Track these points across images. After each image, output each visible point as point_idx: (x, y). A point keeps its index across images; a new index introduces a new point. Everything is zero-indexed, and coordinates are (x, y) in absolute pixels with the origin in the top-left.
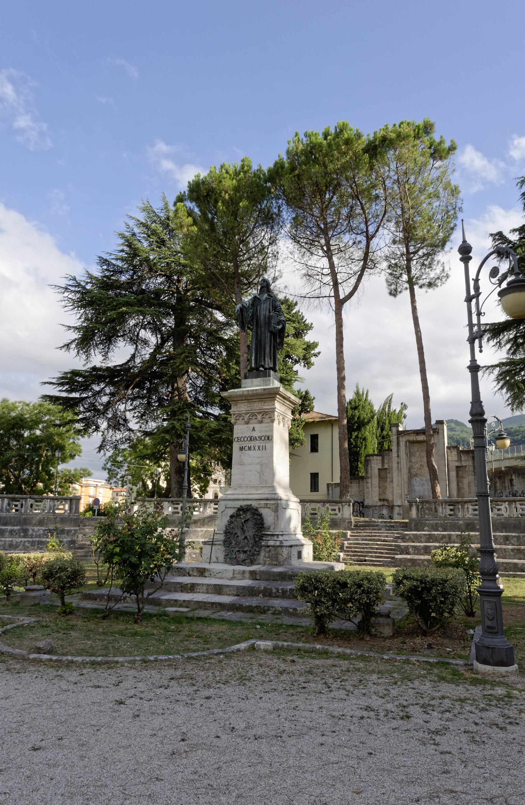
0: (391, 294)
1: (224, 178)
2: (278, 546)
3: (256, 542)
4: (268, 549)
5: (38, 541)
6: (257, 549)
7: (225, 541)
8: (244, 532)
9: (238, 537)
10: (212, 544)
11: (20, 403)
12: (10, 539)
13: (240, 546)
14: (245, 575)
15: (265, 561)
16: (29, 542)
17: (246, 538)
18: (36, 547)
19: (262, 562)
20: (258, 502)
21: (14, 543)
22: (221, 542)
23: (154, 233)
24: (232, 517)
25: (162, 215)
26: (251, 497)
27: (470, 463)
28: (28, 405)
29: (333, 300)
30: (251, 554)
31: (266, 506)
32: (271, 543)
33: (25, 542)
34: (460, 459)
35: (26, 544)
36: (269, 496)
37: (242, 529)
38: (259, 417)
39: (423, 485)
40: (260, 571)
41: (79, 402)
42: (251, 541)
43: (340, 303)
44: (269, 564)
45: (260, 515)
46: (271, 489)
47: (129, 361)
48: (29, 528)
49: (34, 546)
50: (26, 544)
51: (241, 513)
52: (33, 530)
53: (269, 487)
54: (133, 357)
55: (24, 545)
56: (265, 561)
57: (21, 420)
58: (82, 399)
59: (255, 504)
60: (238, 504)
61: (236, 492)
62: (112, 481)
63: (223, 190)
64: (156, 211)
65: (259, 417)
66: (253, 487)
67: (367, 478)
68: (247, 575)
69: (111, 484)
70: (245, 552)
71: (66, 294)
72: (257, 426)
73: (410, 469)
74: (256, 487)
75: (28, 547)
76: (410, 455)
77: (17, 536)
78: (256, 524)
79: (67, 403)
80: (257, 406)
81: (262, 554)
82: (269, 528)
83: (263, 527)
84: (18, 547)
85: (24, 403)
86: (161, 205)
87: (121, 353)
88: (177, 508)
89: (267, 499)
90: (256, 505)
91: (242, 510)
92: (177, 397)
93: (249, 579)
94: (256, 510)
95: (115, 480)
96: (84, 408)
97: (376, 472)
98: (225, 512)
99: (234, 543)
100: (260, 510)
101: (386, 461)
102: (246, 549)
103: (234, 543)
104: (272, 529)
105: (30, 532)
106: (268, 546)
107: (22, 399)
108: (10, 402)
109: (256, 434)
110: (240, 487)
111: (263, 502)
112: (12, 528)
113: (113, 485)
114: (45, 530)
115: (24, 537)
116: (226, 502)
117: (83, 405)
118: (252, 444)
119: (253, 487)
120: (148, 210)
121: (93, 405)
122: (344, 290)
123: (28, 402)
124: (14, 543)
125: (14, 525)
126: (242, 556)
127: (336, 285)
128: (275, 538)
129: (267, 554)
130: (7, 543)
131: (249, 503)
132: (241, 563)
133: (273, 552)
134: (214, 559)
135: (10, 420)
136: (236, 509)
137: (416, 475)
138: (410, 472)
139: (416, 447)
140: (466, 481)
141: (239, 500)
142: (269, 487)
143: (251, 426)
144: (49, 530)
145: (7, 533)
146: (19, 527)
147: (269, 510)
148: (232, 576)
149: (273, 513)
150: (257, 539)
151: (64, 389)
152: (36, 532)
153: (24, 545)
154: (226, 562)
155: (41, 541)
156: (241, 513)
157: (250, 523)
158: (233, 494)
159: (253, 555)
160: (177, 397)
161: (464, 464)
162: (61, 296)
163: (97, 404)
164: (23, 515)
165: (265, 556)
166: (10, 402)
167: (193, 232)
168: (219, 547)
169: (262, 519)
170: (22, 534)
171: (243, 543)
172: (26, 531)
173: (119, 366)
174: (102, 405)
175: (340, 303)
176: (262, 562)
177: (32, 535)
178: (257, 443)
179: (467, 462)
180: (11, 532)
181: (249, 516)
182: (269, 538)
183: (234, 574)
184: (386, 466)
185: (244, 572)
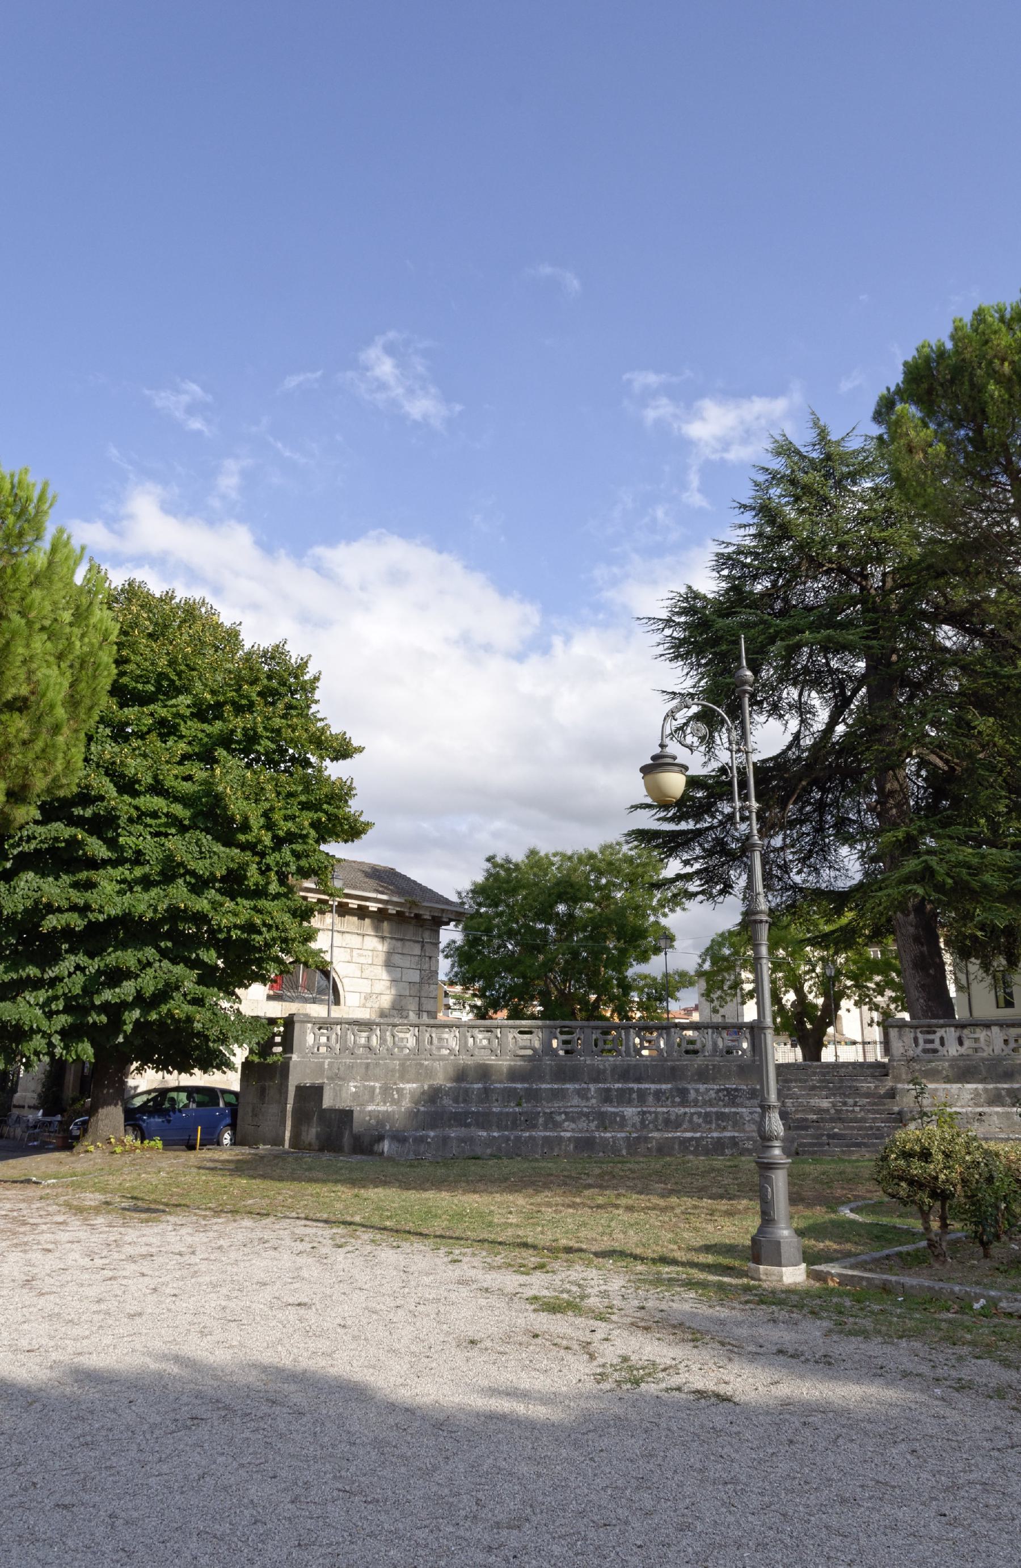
1: (995, 332)
5: (717, 1113)
11: (555, 855)
12: (665, 1110)
16: (699, 1114)
18: (714, 1126)
21: (673, 1117)
23: (808, 490)
25: (814, 455)
28: (570, 858)
33: (692, 1114)
35: (695, 1118)
41: (692, 840)
47: (789, 747)
48: (689, 1086)
49: (710, 1122)
50: (695, 1118)
52: (697, 1091)
54: (797, 737)
55: (691, 1121)
57: (572, 885)
58: (698, 833)
62: (714, 996)
63: (995, 356)
64: (803, 450)
69: (712, 1001)
71: (668, 632)
75: (699, 1125)
77: (669, 1103)
79: (670, 842)
84: (680, 1125)
85: (563, 855)
86: (811, 435)
87: (770, 736)
88: (932, 1041)
92: (894, 811)
95: (719, 993)
96: (704, 850)
105: (692, 1095)
107: (560, 849)
108: (542, 854)
112: (658, 1086)
113: (716, 1003)
114: (719, 1091)
115: (684, 1103)
117: (700, 845)
120: (785, 449)
121: (720, 843)
123: (569, 853)
124: (673, 1117)
125: (659, 1082)
130: (661, 1117)
135: (549, 888)
144: (726, 1089)
145: (651, 1098)
146: (669, 1086)
151: (670, 814)
152: (702, 1095)
155: (723, 1113)
160: (894, 811)
162: (658, 637)
163: (729, 839)
164: (666, 1060)
166: (542, 854)
167: (937, 456)
170: (677, 1099)
172: (683, 1093)
173: (771, 759)
174: (738, 840)
177: (696, 1101)
180: (658, 1094)
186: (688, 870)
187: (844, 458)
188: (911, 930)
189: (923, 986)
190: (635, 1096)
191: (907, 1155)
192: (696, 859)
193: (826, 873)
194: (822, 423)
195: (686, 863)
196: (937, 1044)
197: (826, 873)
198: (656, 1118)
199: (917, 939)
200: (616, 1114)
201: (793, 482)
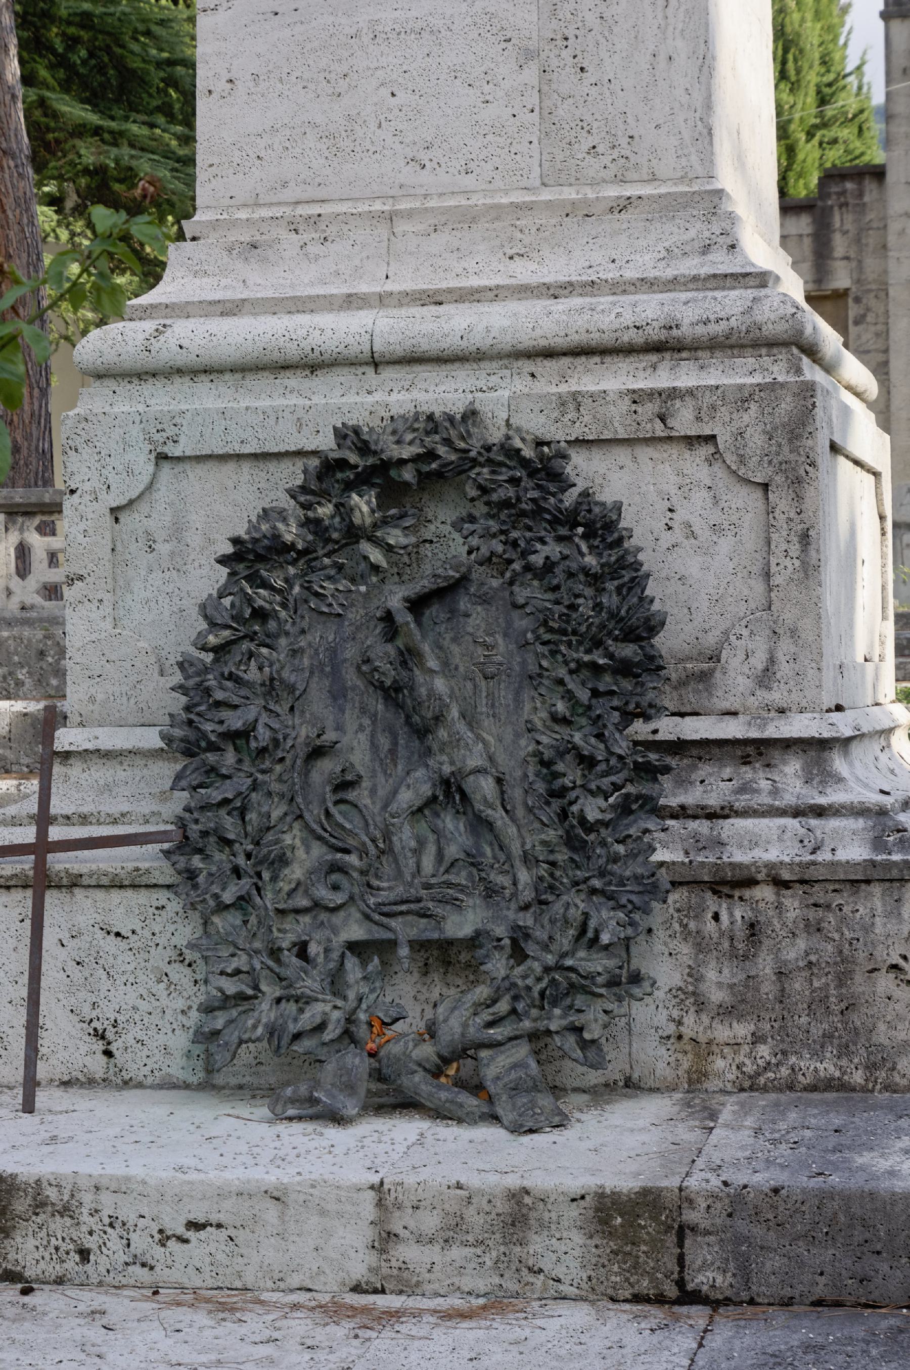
2: (858, 880)
3: (578, 836)
4: (734, 915)
6: (609, 923)
7: (185, 843)
8: (422, 732)
9: (344, 785)
10: (41, 883)
13: (389, 890)
14: (537, 1243)
15: (703, 1050)
17: (451, 792)
19: (655, 1057)
20: (551, 381)
22: (146, 858)
24: (249, 557)
26: (457, 325)
30: (530, 974)
31: (659, 428)
32: (763, 842)
36: (690, 312)
37: (392, 693)
40: (736, 1201)
42: (525, 834)
44: (750, 1085)
45: (600, 526)
46: (697, 230)
51: (363, 505)
53: (670, 207)
56: (703, 1050)
59: (515, 406)
60: (314, 415)
61: (262, 282)
66: (468, 218)
68: (566, 1250)
70: (444, 957)
74: (507, 222)
78: (556, 632)
81: (664, 964)
82: (704, 673)
83: (652, 665)
89: (664, 346)
90: (536, 423)
93: (599, 1294)
94: (545, 467)
98: (154, 518)
99: (304, 858)
100: (584, 468)
101: (840, 245)
102: (461, 925)
103: (304, 858)
104: (735, 680)
106: (732, 883)
110: (312, 226)
111: (616, 379)
116: (161, 399)
119: (468, 218)
126: (416, 1009)
128: (791, 780)
129: (717, 981)
131: (443, 393)
132: (418, 1083)
133: (794, 952)
134: (66, 1045)
136: (292, 474)
141: (313, 365)
142: (670, 207)
147: (694, 464)
148: (359, 1267)
149: (746, 501)
150: (592, 809)
154: (212, 1071)
156: (363, 505)
157: (477, 619)
158: (230, 309)
159: (566, 988)
165: (692, 996)
168: (123, 909)
169: (623, 571)
171: (424, 852)
176: (655, 1057)
181: (446, 537)
182: (712, 786)
183: (385, 1240)
184: (841, 279)
185: (519, 1213)
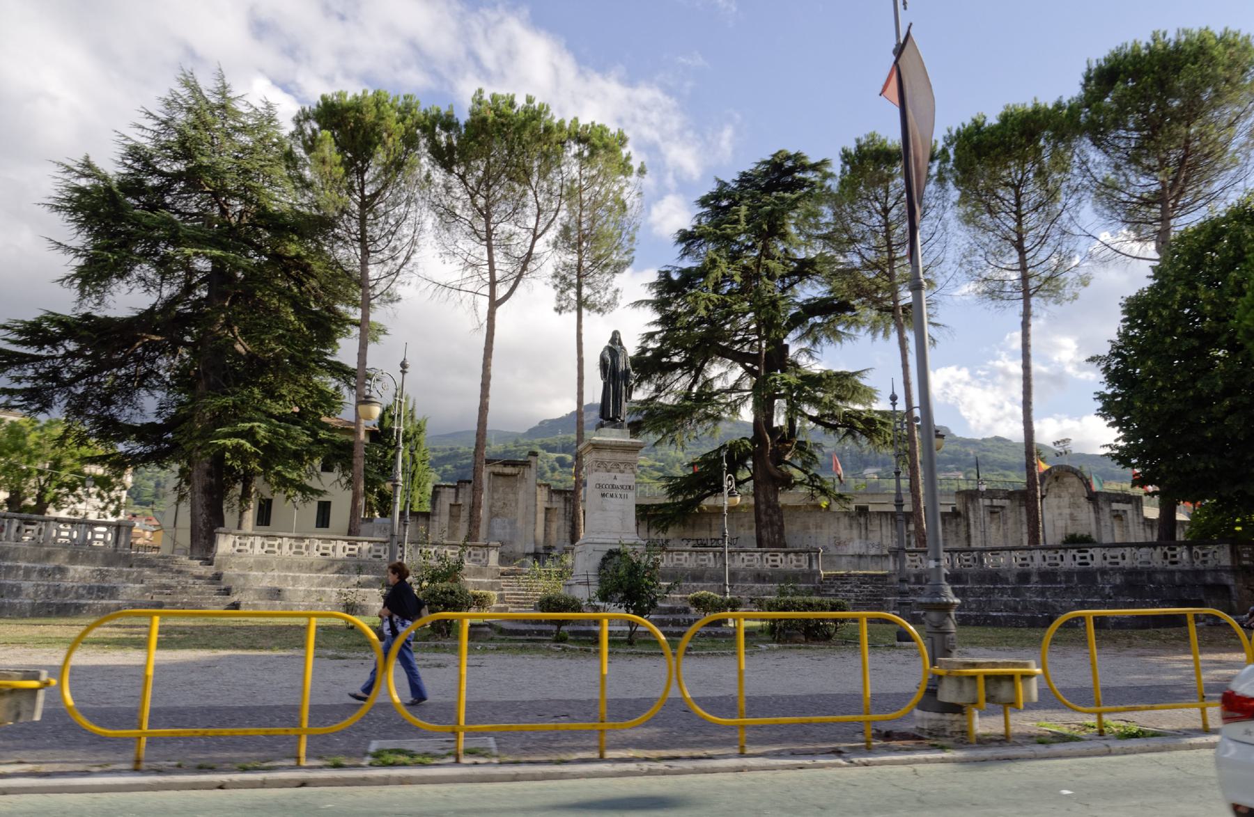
0: (556, 310)
27: (562, 505)
29: (487, 300)
34: (550, 500)
38: (622, 467)
39: (504, 528)
43: (494, 304)
50: (81, 590)
52: (76, 570)
55: (76, 592)
60: (608, 548)
65: (622, 467)
67: (434, 514)
72: (619, 475)
73: (491, 507)
76: (493, 490)
80: (620, 456)
91: (611, 554)
97: (447, 508)
109: (617, 483)
118: (614, 492)
121: (56, 371)
122: (501, 291)
127: (493, 283)
137: (497, 515)
138: (491, 511)
139: (500, 481)
140: (554, 526)
143: (613, 474)
145: (35, 574)
153: (76, 592)
161: (555, 505)
175: (494, 304)
177: (73, 577)
178: (619, 492)
179: (558, 503)
184: (460, 502)
186: (16, 386)
187: (236, 114)
188: (207, 466)
189: (208, 506)
190: (21, 572)
191: (445, 593)
192: (27, 379)
193: (128, 411)
194: (227, 82)
195: (18, 380)
196: (248, 547)
197: (128, 411)
198: (48, 590)
199: (209, 473)
200: (13, 586)
201: (198, 116)
